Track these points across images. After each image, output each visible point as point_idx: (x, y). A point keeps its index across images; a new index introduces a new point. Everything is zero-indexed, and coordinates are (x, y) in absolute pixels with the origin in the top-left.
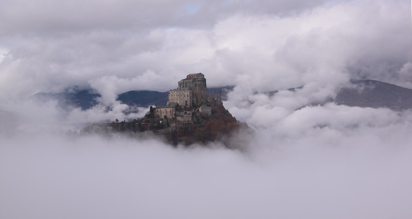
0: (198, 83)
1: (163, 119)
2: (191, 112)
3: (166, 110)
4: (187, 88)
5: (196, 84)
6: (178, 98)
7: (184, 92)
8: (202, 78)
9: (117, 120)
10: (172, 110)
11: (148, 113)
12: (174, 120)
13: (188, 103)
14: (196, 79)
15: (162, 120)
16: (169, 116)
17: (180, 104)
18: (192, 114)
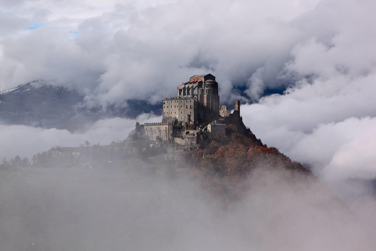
0: (206, 88)
1: (154, 141)
2: (195, 132)
3: (159, 128)
4: (190, 96)
5: (203, 91)
6: (177, 111)
7: (185, 102)
8: (212, 82)
9: (87, 143)
10: (167, 128)
11: (132, 132)
12: (170, 142)
13: (192, 118)
14: (203, 83)
15: (153, 142)
16: (165, 139)
17: (179, 120)
18: (197, 133)
